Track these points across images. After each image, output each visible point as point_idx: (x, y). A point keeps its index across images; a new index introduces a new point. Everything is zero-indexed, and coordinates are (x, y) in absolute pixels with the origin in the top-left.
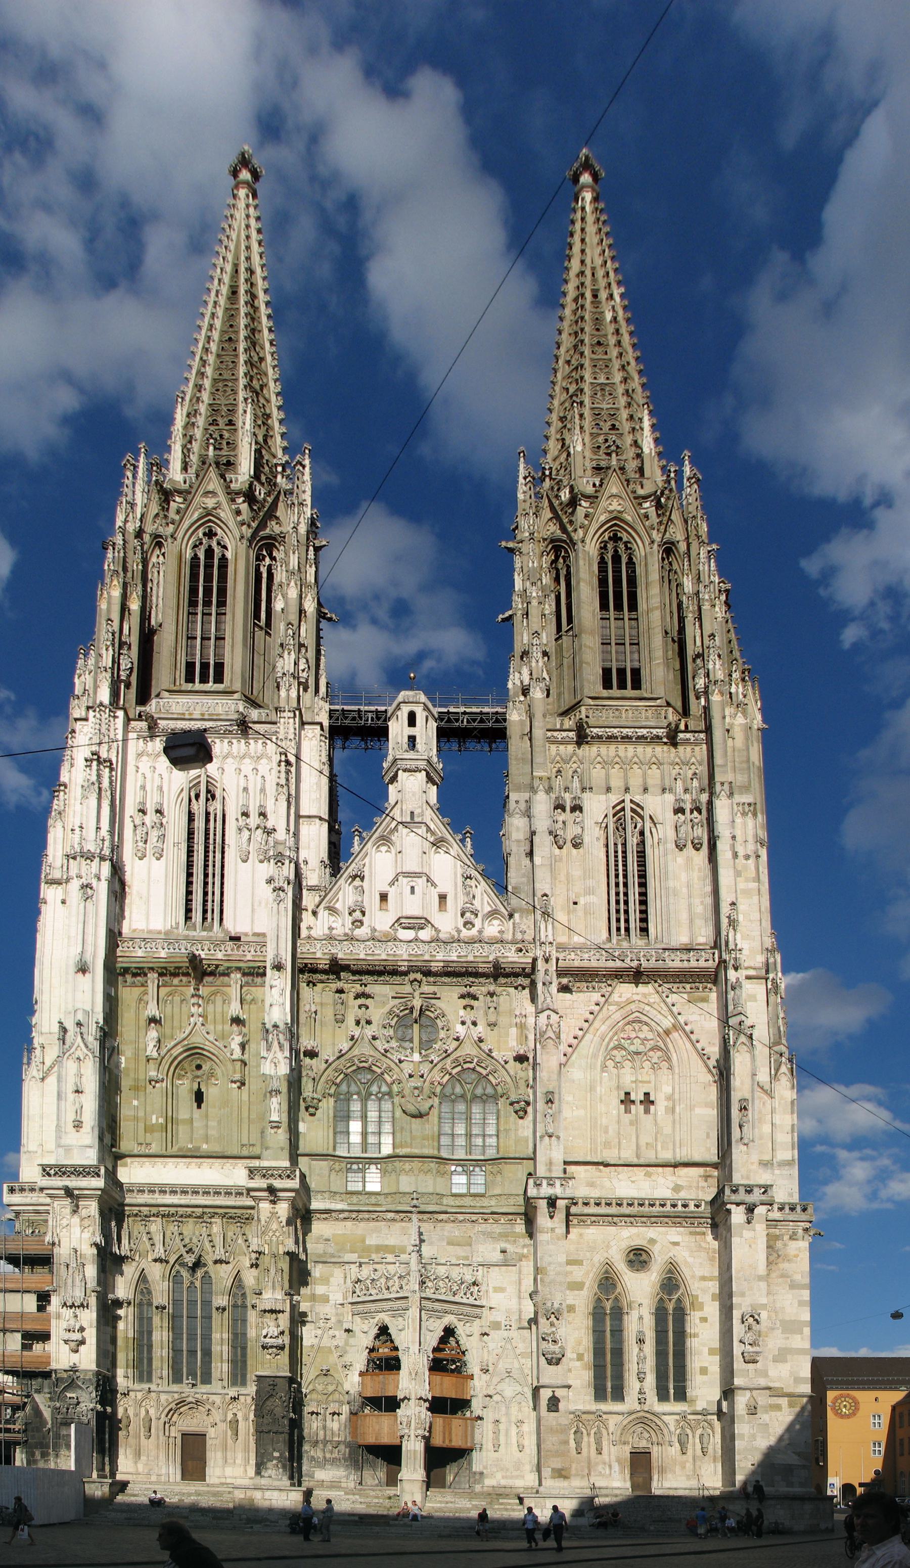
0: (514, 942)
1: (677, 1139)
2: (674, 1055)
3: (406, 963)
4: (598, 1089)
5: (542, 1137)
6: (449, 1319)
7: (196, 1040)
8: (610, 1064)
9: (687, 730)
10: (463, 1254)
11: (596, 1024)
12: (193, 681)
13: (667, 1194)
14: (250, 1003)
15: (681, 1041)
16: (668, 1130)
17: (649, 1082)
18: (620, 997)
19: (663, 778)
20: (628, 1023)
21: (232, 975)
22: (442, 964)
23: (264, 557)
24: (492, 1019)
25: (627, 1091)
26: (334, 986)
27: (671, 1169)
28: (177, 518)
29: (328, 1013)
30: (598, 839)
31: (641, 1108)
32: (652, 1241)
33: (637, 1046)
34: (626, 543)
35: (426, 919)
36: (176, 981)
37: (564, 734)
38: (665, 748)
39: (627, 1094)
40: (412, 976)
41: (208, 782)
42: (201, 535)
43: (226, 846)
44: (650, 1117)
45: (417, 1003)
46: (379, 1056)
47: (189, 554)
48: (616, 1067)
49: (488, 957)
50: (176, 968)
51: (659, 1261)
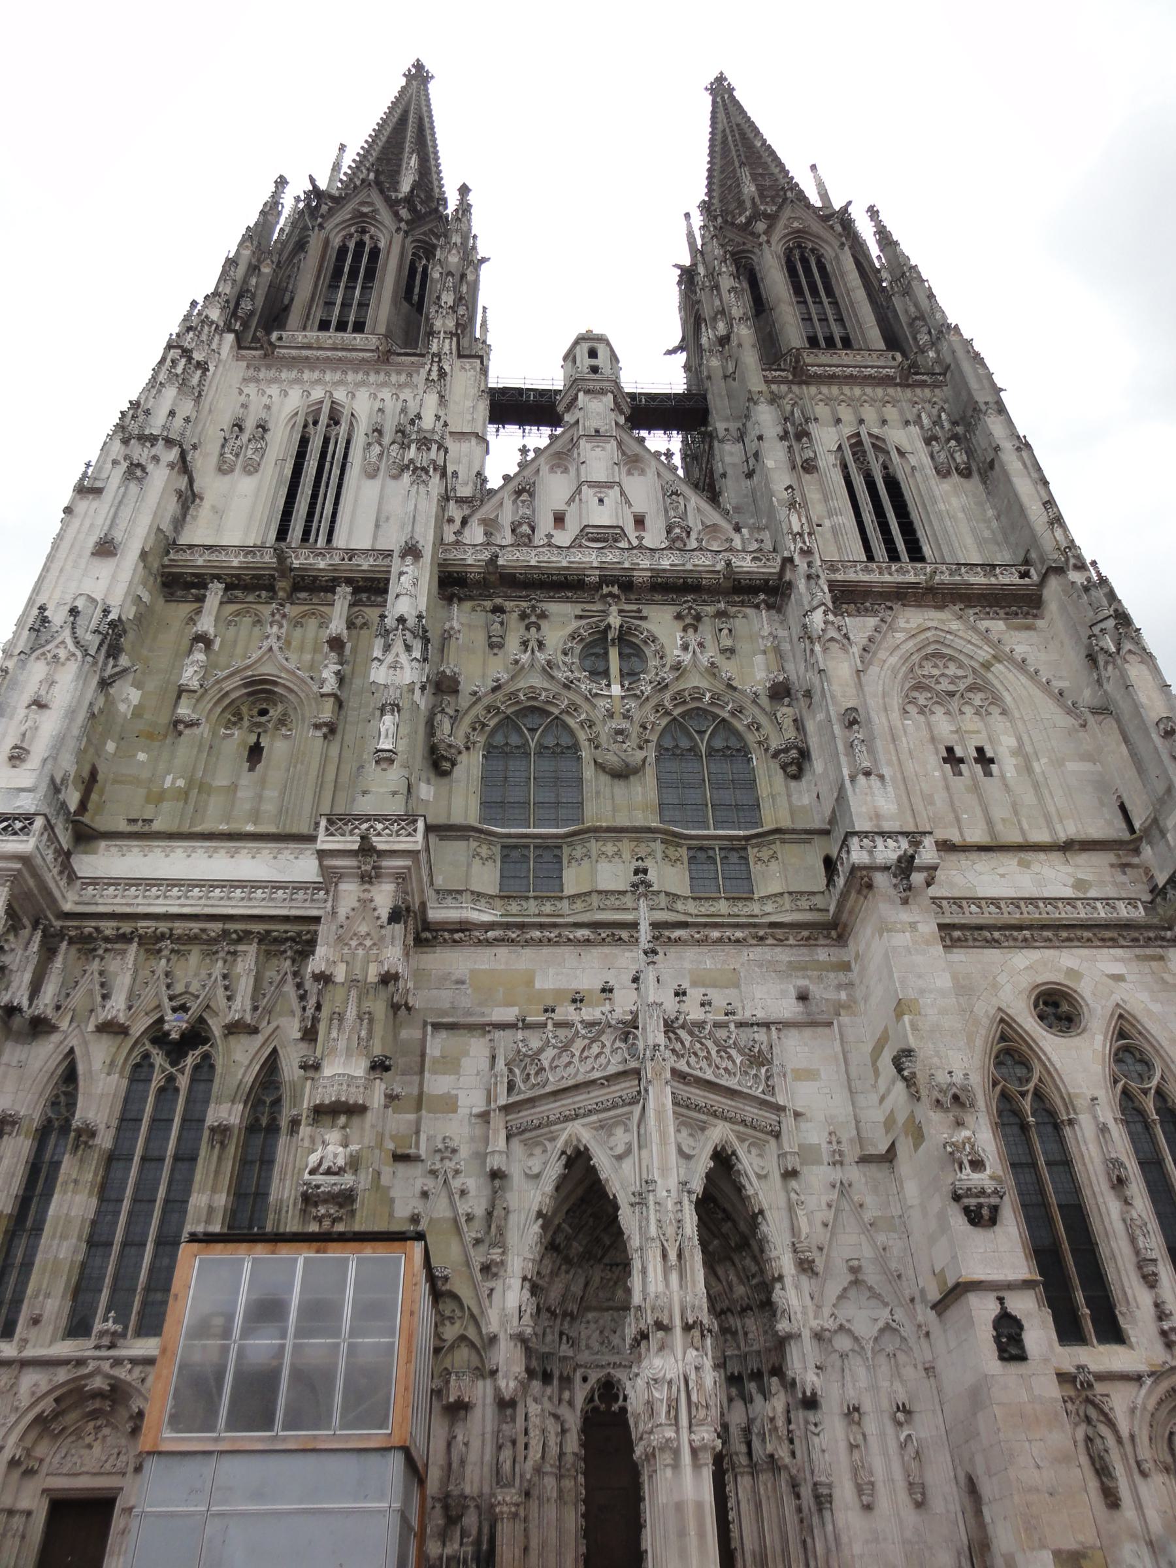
1: (1052, 809)
2: (1005, 694)
3: (597, 572)
4: (904, 739)
5: (853, 779)
6: (719, 1133)
7: (267, 669)
8: (912, 709)
11: (882, 654)
14: (361, 628)
15: (1010, 676)
17: (978, 732)
18: (907, 622)
19: (902, 412)
20: (926, 657)
21: (338, 589)
23: (420, 258)
24: (727, 642)
25: (949, 744)
26: (488, 604)
27: (1056, 857)
29: (480, 638)
30: (834, 465)
31: (978, 768)
32: (1071, 972)
33: (945, 685)
34: (812, 250)
35: (622, 528)
36: (251, 598)
38: (899, 389)
39: (950, 750)
40: (605, 590)
42: (353, 229)
43: (349, 465)
45: (615, 620)
46: (555, 688)
47: (336, 242)
49: (713, 566)
50: (254, 577)
51: (1099, 1011)
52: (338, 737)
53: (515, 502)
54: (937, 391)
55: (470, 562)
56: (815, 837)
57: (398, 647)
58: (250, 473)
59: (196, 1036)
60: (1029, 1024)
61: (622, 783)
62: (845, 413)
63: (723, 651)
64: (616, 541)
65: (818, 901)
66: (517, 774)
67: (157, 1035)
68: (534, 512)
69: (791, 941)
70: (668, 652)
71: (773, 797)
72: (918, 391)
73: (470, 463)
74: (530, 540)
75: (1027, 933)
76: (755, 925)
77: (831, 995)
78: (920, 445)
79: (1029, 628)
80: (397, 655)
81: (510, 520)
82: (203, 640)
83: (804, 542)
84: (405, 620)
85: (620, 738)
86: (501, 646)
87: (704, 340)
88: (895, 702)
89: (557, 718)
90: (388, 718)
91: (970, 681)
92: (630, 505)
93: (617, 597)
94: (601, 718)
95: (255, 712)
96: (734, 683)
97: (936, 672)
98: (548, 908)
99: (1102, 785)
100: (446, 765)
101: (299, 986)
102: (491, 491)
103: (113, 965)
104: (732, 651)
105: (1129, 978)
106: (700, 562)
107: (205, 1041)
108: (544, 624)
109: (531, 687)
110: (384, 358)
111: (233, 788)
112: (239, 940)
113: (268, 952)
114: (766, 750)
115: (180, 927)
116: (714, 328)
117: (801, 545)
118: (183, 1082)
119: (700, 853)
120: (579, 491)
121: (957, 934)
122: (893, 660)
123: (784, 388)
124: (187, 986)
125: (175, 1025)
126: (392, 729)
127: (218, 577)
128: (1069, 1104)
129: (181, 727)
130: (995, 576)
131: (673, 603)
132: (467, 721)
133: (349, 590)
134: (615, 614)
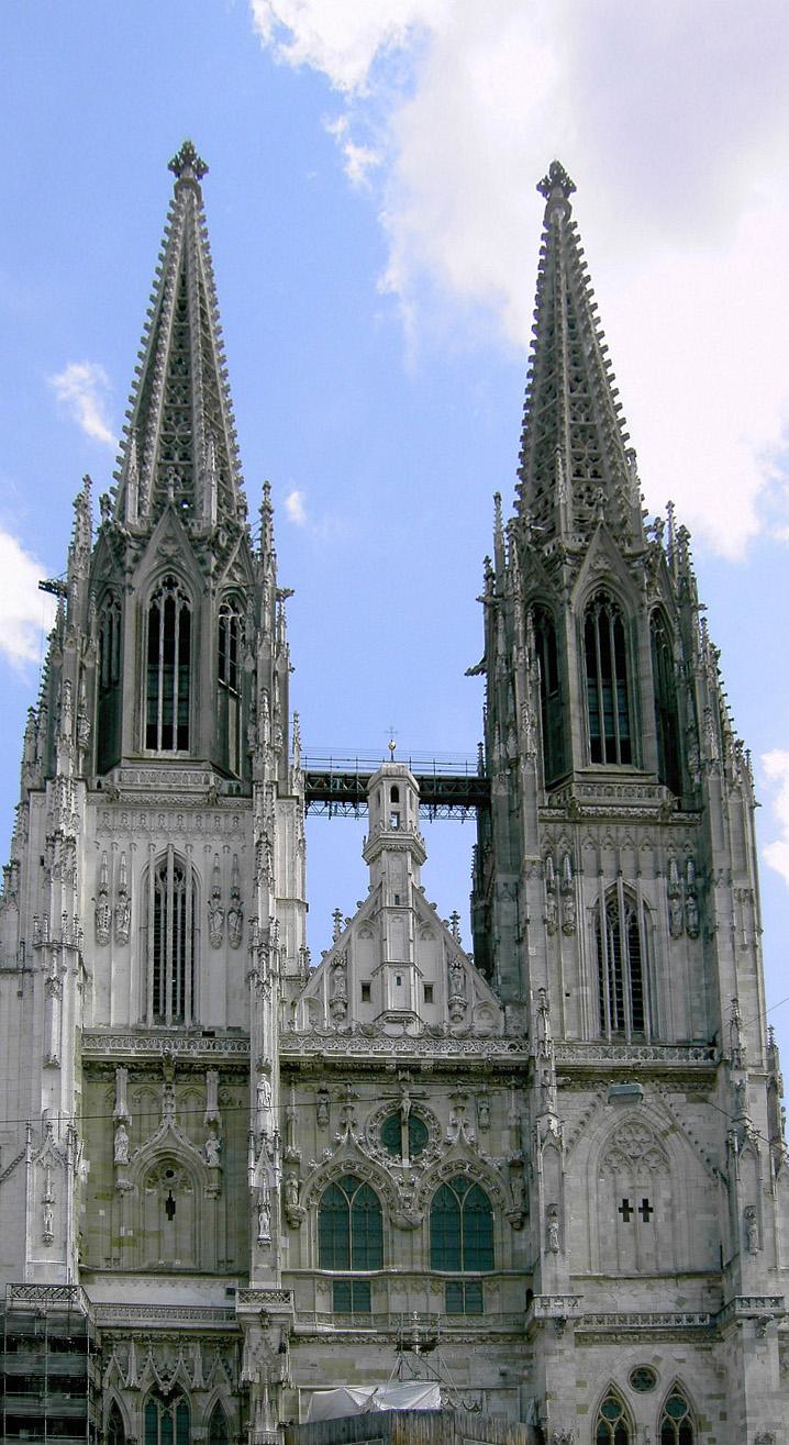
0: (507, 1037)
2: (672, 1157)
7: (169, 1144)
8: (606, 1170)
9: (680, 811)
10: (461, 1378)
11: (593, 1126)
12: (156, 748)
13: (671, 1307)
15: (678, 1143)
16: (667, 1239)
17: (647, 1188)
19: (656, 861)
24: (485, 1121)
28: (133, 566)
36: (145, 1080)
37: (554, 812)
38: (658, 828)
39: (625, 1202)
41: (175, 860)
44: (649, 1225)
45: (406, 1105)
47: (147, 607)
48: (613, 1172)
50: (148, 1064)
52: (223, 1197)
54: (691, 829)
55: (302, 1054)
58: (122, 945)
59: (176, 1391)
60: (625, 1387)
61: (408, 1234)
62: (608, 864)
65: (519, 1317)
67: (155, 1391)
69: (501, 1342)
71: (503, 1243)
72: (675, 830)
75: (637, 1336)
76: (481, 1334)
77: (519, 1373)
78: (663, 901)
79: (704, 1100)
82: (121, 1121)
85: (407, 1205)
87: (496, 757)
88: (594, 1168)
91: (652, 1146)
95: (164, 1175)
97: (629, 1138)
98: (362, 1321)
99: (714, 1232)
101: (226, 1367)
102: (313, 969)
103: (123, 1353)
104: (488, 1127)
105: (687, 1361)
107: (181, 1393)
108: (356, 1105)
110: (213, 801)
111: (159, 1234)
112: (189, 1341)
113: (205, 1347)
115: (156, 1334)
116: (505, 743)
118: (174, 1415)
119: (453, 1287)
121: (597, 1337)
122: (600, 1131)
123: (559, 827)
124: (166, 1366)
125: (165, 1388)
127: (122, 1064)
128: (635, 1428)
129: (122, 1191)
130: (687, 1058)
133: (216, 1074)
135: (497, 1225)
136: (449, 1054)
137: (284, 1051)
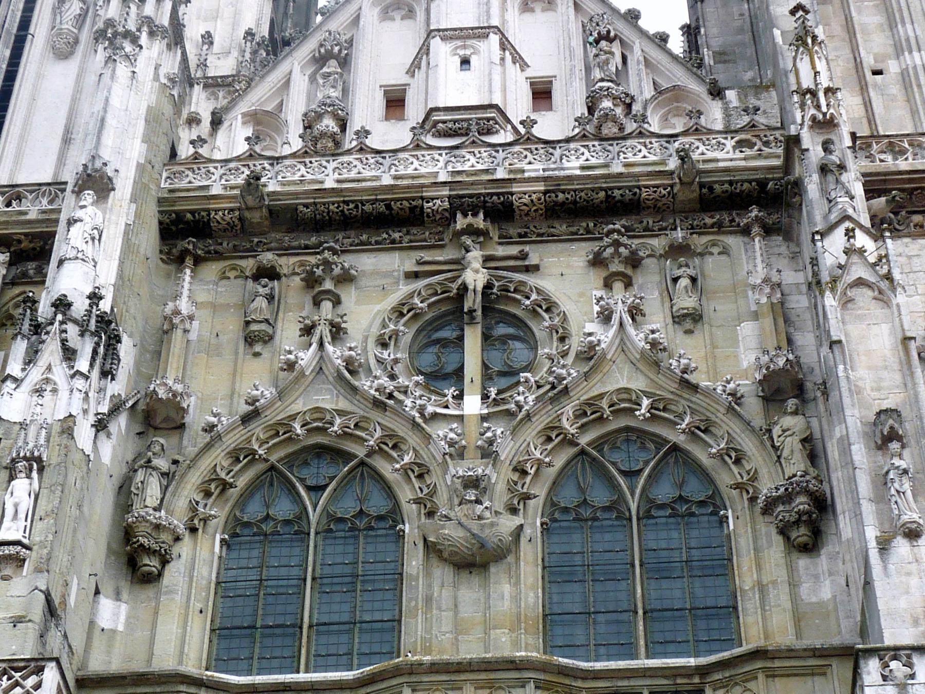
3: (446, 192)
5: (884, 546)
22: (541, 187)
24: (687, 302)
26: (249, 265)
29: (232, 327)
40: (461, 222)
46: (359, 410)
49: (663, 162)
53: (313, 79)
55: (216, 190)
56: (834, 662)
57: (51, 352)
61: (475, 580)
63: (678, 319)
64: (489, 132)
66: (284, 572)
68: (345, 91)
70: (573, 327)
71: (762, 588)
73: (237, 15)
74: (337, 144)
80: (49, 368)
81: (302, 109)
83: (818, 107)
84: (70, 305)
85: (471, 495)
86: (268, 339)
89: (362, 463)
90: (21, 486)
92: (524, 65)
93: (485, 233)
94: (439, 458)
96: (692, 378)
100: (151, 563)
106: (638, 158)
108: (349, 296)
109: (317, 409)
114: (753, 500)
117: (813, 111)
120: (425, 49)
126: (26, 503)
131: (589, 236)
132: (195, 478)
134: (477, 265)
135: (743, 543)
136: (583, 168)
137: (171, 191)
